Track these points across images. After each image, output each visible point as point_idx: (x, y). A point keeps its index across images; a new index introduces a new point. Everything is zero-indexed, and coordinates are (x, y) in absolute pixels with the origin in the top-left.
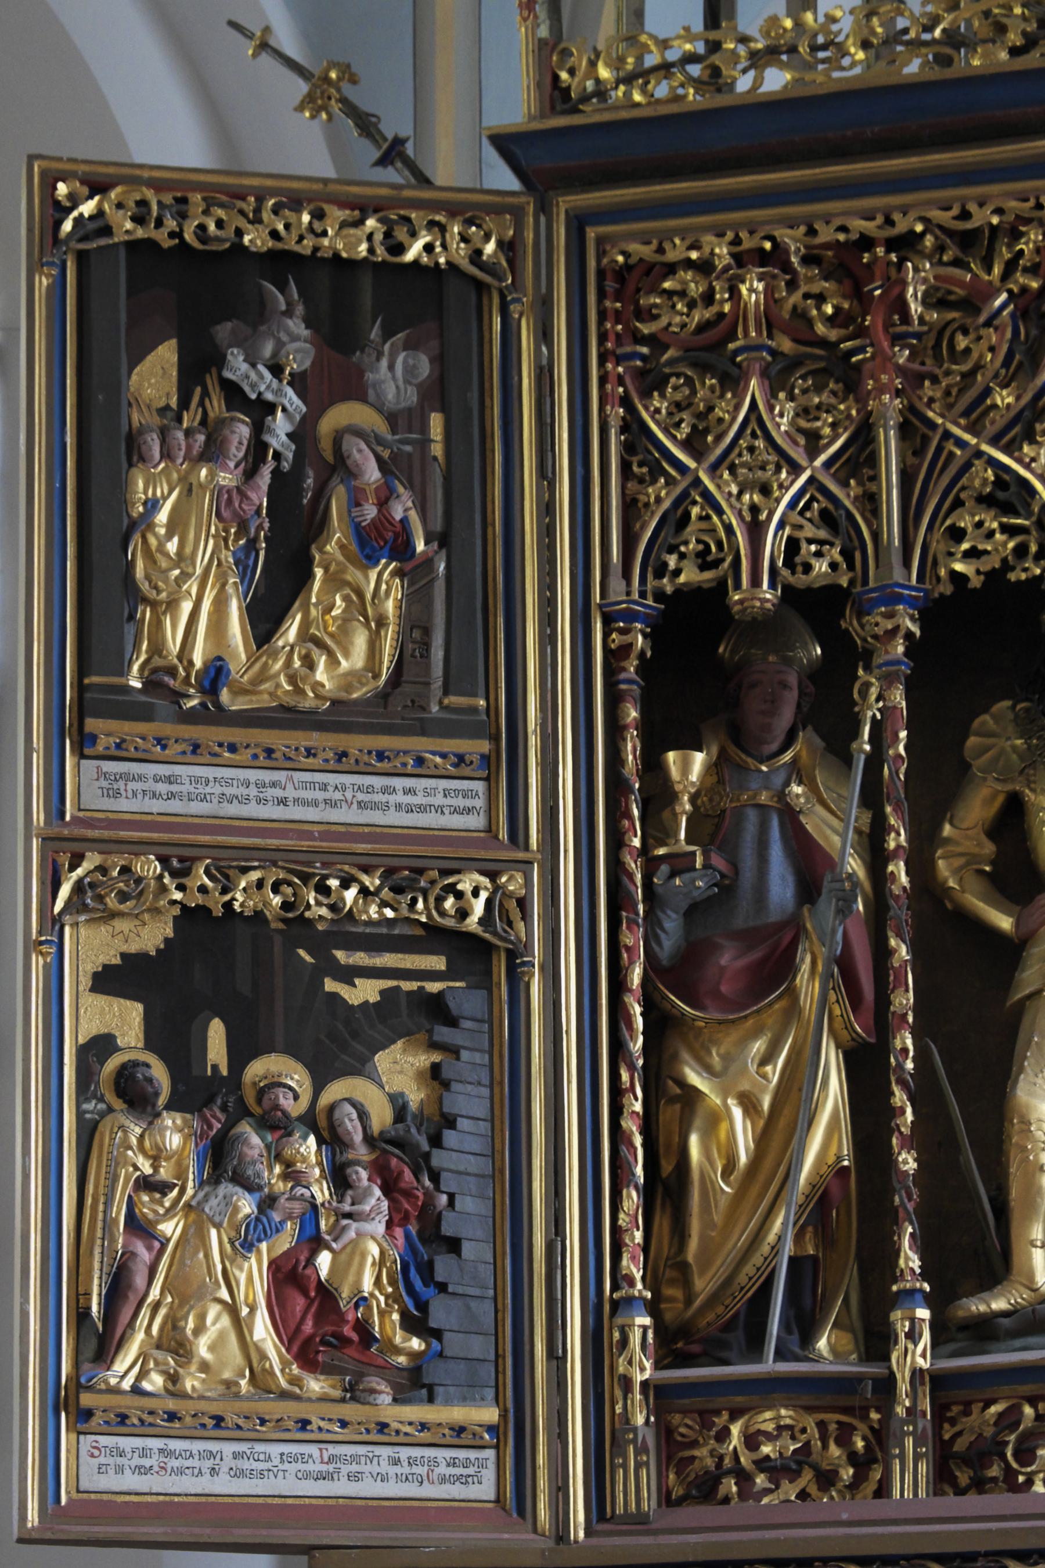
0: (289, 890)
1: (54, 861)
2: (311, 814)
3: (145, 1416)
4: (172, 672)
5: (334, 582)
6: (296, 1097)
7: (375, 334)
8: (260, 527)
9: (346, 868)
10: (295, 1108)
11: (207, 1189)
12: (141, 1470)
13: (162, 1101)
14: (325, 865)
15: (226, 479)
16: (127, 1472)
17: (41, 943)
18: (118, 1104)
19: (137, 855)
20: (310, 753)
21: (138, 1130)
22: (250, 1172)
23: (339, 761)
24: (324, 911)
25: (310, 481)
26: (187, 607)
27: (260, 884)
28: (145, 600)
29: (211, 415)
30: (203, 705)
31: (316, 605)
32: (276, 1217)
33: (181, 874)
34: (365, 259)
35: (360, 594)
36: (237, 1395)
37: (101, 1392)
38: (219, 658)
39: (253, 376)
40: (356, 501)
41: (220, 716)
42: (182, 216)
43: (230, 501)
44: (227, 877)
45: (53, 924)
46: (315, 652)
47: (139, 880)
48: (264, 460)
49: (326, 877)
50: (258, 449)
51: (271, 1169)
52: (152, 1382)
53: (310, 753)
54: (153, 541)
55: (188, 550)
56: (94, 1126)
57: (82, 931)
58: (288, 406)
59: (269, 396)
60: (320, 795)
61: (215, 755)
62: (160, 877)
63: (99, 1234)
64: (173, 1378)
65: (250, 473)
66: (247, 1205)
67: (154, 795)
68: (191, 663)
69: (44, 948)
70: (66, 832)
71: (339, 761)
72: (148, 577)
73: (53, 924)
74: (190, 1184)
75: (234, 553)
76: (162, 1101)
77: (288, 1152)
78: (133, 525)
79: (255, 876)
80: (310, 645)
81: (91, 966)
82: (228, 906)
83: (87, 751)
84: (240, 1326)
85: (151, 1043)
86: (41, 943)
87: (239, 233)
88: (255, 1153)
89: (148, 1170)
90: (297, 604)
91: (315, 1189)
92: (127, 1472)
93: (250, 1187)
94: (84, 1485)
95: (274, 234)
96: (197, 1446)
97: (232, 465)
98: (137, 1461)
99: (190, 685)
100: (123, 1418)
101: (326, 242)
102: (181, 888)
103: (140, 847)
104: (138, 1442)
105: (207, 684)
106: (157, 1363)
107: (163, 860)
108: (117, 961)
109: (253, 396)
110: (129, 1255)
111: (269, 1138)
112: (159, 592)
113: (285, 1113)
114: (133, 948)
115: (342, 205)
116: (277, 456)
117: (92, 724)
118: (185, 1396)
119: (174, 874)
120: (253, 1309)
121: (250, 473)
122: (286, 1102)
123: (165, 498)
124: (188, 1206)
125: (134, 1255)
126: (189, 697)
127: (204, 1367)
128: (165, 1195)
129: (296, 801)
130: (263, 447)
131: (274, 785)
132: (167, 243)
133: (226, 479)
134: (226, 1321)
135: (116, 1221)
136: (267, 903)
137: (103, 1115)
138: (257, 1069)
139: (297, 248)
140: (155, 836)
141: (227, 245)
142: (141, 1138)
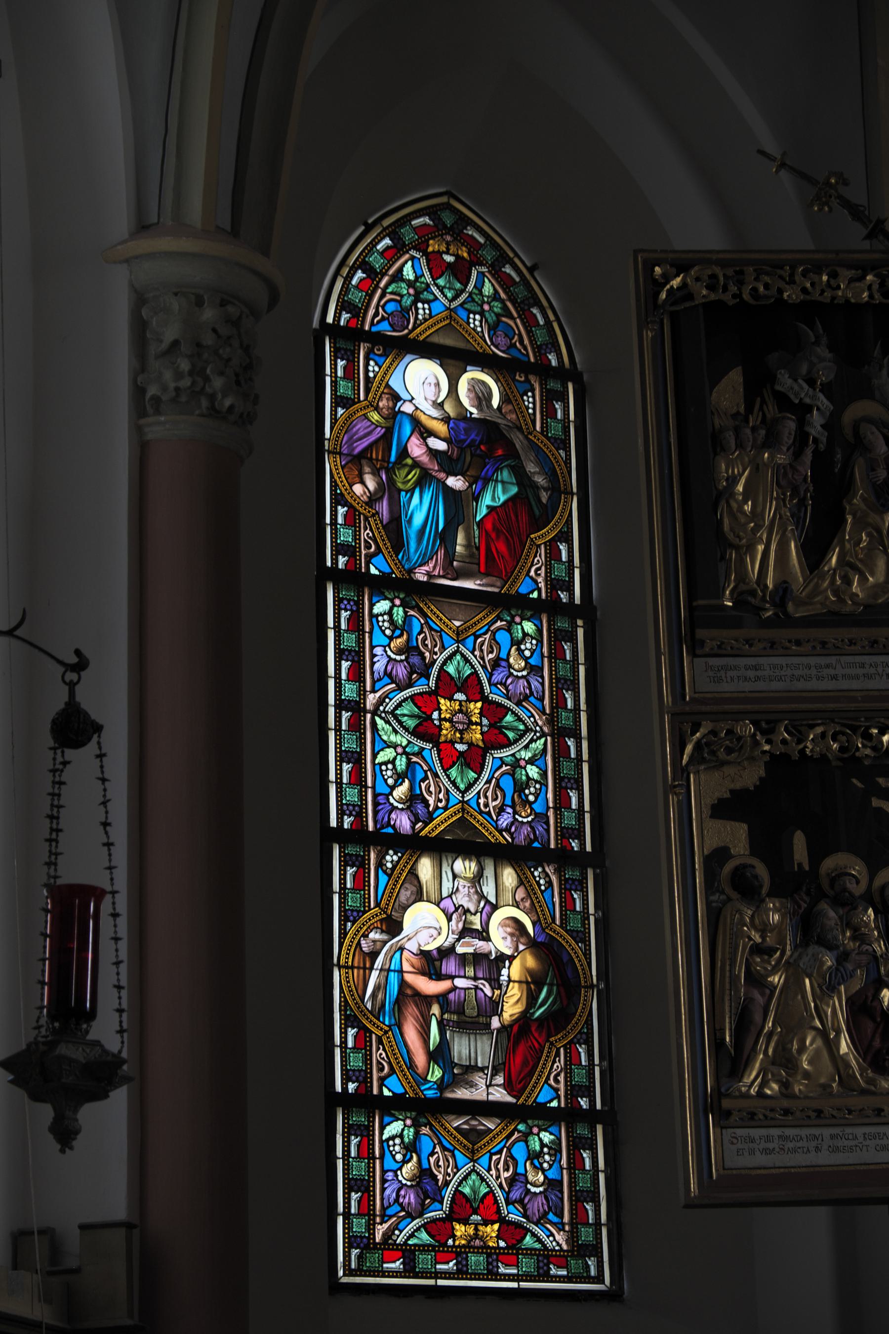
0: (844, 738)
1: (680, 729)
2: (855, 685)
3: (768, 1113)
4: (753, 593)
5: (861, 524)
6: (858, 882)
7: (877, 353)
8: (807, 490)
9: (882, 720)
10: (858, 890)
11: (800, 950)
12: (767, 1151)
13: (764, 891)
14: (867, 719)
15: (782, 458)
16: (758, 1153)
17: (675, 787)
18: (734, 895)
19: (737, 721)
20: (852, 642)
21: (750, 912)
22: (829, 937)
23: (872, 646)
24: (868, 751)
25: (839, 456)
26: (760, 548)
27: (823, 735)
28: (732, 546)
29: (768, 416)
30: (775, 614)
31: (849, 541)
32: (850, 966)
33: (768, 732)
34: (867, 302)
35: (879, 531)
36: (831, 1094)
37: (736, 1097)
38: (785, 582)
39: (796, 387)
40: (872, 467)
41: (788, 622)
42: (741, 283)
43: (785, 474)
44: (800, 732)
45: (682, 772)
46: (851, 573)
47: (739, 738)
48: (806, 444)
49: (868, 728)
50: (802, 438)
51: (844, 934)
52: (771, 1089)
53: (852, 642)
54: (734, 505)
55: (759, 509)
56: (719, 911)
57: (702, 776)
58: (820, 405)
59: (807, 401)
60: (860, 671)
61: (787, 648)
62: (754, 735)
63: (727, 986)
64: (785, 1085)
65: (798, 454)
66: (829, 962)
67: (746, 679)
68: (766, 586)
69: (677, 790)
70: (687, 709)
71: (872, 646)
72: (732, 529)
73: (682, 772)
74: (788, 947)
75: (790, 509)
76: (764, 891)
77: (855, 921)
78: (720, 495)
79: (819, 730)
80: (847, 569)
81: (709, 801)
82: (802, 752)
83: (698, 652)
84: (831, 1046)
85: (754, 852)
86: (675, 787)
87: (780, 291)
88: (832, 923)
89: (758, 940)
90: (836, 541)
91: (875, 946)
92: (758, 1153)
93: (830, 947)
94: (728, 1164)
95: (804, 290)
96: (804, 1132)
97: (785, 449)
98: (763, 1145)
99: (767, 602)
100: (752, 1115)
101: (840, 293)
102: (769, 742)
103: (738, 716)
104: (763, 1132)
105: (777, 599)
106: (773, 1075)
107: (755, 723)
108: (727, 795)
109: (797, 401)
110: (749, 1000)
111: (841, 912)
112: (740, 539)
113: (850, 893)
114: (738, 786)
115: (850, 267)
116: (815, 440)
117: (700, 633)
118: (794, 1097)
119: (764, 733)
120: (838, 1032)
121: (798, 454)
122: (851, 886)
123: (741, 475)
124: (788, 962)
125: (752, 1000)
126: (766, 610)
127: (806, 1075)
128: (771, 956)
129: (843, 676)
130: (807, 434)
131: (828, 666)
132: (732, 302)
133: (782, 458)
134: (819, 1042)
135: (739, 977)
136: (829, 748)
137: (724, 903)
138: (829, 864)
139: (820, 299)
140: (749, 707)
141: (773, 300)
142: (752, 918)
